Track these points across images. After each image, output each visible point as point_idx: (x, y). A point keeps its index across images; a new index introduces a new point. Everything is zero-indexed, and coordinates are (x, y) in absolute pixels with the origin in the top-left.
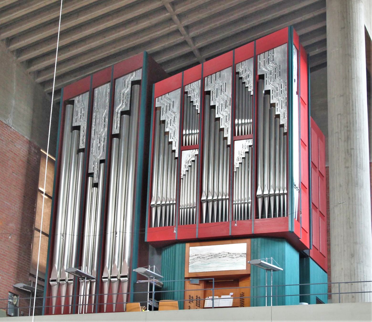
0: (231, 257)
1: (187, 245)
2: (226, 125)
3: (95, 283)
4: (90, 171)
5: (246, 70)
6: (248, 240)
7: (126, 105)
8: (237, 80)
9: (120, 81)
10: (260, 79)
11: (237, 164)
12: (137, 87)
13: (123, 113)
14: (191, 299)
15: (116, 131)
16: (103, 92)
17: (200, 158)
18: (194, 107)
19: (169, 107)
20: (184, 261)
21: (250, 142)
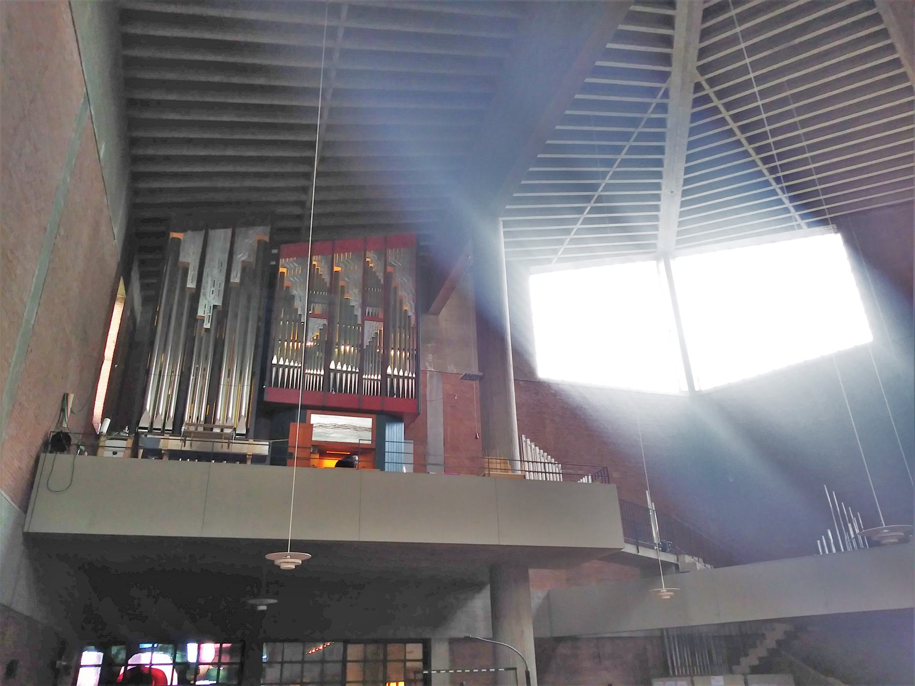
6: (374, 416)
7: (249, 256)
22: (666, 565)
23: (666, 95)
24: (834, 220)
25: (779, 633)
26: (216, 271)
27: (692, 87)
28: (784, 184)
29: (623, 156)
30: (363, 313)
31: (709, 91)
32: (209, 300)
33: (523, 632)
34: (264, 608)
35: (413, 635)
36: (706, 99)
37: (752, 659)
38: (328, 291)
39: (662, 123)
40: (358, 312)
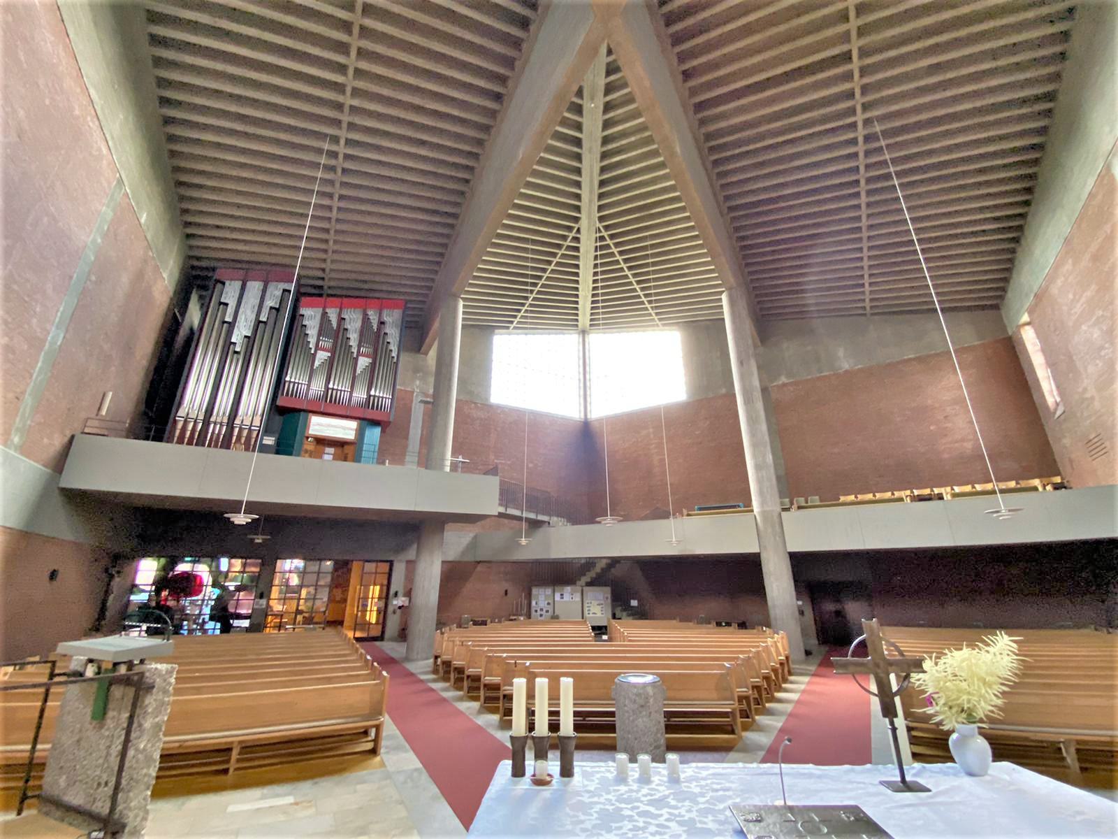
0: (344, 429)
1: (310, 414)
2: (354, 343)
4: (233, 340)
7: (276, 303)
8: (366, 320)
11: (358, 371)
13: (271, 308)
14: (306, 451)
15: (263, 318)
16: (254, 287)
19: (311, 317)
20: (306, 425)
21: (370, 360)
22: (543, 522)
23: (578, 231)
25: (603, 564)
26: (249, 312)
29: (552, 267)
31: (605, 234)
33: (433, 562)
34: (260, 541)
36: (602, 239)
38: (338, 335)
39: (577, 249)
40: (355, 350)
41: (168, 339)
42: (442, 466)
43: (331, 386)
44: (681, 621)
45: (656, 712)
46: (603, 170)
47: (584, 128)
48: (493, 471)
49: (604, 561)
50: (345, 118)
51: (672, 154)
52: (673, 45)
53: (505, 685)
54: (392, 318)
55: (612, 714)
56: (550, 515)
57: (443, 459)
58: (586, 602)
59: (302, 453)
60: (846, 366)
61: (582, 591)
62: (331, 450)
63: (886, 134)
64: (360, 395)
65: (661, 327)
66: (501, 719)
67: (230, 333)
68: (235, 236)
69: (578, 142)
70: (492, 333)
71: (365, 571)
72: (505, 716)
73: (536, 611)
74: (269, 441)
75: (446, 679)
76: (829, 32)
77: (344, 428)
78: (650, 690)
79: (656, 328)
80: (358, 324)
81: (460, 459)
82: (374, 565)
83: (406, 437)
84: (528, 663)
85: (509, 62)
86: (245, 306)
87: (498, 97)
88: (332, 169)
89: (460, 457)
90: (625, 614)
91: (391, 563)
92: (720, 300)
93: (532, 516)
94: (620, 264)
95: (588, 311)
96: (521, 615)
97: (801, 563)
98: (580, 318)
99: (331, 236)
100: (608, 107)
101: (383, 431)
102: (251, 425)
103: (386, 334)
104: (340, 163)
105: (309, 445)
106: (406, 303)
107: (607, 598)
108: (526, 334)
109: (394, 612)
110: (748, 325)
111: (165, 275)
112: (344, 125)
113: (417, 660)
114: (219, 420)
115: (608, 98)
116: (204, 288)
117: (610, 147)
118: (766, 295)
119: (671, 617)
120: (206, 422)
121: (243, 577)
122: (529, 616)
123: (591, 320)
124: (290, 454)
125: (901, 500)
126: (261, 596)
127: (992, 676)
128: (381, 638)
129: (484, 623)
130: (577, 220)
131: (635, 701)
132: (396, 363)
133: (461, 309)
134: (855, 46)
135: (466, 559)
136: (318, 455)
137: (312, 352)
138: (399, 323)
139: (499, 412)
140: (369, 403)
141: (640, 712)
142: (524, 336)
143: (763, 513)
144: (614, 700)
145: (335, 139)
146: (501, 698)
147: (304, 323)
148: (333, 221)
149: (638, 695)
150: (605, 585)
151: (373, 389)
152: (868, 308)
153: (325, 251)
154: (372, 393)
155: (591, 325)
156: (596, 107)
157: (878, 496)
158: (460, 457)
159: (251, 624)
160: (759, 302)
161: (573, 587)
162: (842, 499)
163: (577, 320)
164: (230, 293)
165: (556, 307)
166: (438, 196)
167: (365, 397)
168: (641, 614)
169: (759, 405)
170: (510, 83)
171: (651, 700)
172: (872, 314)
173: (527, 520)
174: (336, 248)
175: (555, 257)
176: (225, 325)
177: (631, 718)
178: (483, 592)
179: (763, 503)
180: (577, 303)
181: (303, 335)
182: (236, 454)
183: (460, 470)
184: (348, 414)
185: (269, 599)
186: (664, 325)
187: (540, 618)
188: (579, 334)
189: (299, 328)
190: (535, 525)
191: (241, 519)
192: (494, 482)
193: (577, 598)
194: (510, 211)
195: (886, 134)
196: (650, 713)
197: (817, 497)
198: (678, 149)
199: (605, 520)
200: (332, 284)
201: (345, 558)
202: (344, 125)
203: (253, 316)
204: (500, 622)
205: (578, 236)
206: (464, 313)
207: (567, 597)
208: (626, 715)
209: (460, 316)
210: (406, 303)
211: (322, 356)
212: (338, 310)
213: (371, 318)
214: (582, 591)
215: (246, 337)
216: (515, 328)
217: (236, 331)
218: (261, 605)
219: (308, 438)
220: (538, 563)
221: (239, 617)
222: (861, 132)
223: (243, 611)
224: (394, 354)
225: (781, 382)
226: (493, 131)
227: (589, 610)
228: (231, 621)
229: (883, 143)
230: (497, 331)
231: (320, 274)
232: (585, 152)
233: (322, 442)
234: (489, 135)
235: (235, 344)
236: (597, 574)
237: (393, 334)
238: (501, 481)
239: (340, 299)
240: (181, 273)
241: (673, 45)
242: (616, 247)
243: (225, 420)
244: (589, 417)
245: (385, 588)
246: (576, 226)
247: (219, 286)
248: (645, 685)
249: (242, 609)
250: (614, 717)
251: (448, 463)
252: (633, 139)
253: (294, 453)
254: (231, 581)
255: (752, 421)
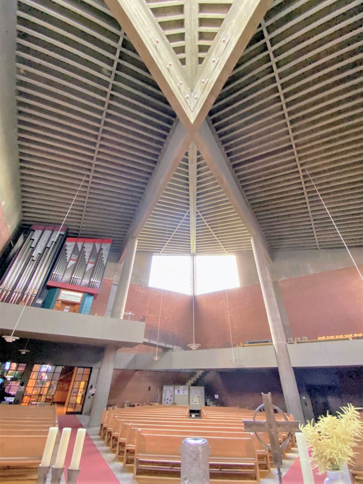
0: (76, 297)
1: (61, 289)
2: (87, 258)
3: (9, 292)
4: (33, 255)
5: (98, 246)
6: (83, 293)
9: (55, 232)
10: (101, 249)
11: (87, 270)
12: (61, 236)
14: (56, 307)
15: (48, 246)
16: (47, 233)
17: (76, 264)
18: (31, 240)
19: (70, 246)
20: (59, 294)
21: (93, 265)
22: (169, 349)
23: (189, 213)
24: (233, 252)
25: (200, 373)
26: (43, 243)
27: (196, 212)
28: (221, 241)
29: (178, 227)
30: (89, 261)
31: (200, 214)
32: (39, 250)
34: (24, 353)
35: (87, 366)
37: (191, 381)
38: (80, 254)
39: (189, 220)
40: (87, 261)
41: (5, 254)
42: (119, 316)
43: (73, 277)
44: (240, 407)
45: (203, 464)
46: (198, 189)
47: (189, 174)
48: (143, 320)
49: (201, 372)
50: (93, 168)
51: (222, 182)
52: (222, 144)
53: (128, 443)
54: (106, 247)
55: (179, 465)
56: (173, 345)
57: (120, 313)
58: (191, 395)
59: (55, 308)
60: (312, 272)
61: (189, 388)
62: (69, 307)
63: (312, 175)
64: (86, 281)
65: (227, 253)
66: (124, 465)
67: (33, 251)
68: (42, 212)
69: (187, 179)
70: (152, 255)
71: (78, 373)
72: (127, 463)
73: (165, 400)
74: (40, 302)
75: (103, 439)
76: (282, 139)
77: (76, 297)
78: (200, 449)
79: (224, 254)
80: (90, 249)
81: (130, 313)
82: (82, 369)
83: (107, 303)
84: (140, 429)
85: (159, 150)
86: (42, 240)
87: (155, 162)
88: (86, 187)
89: (130, 312)
90: (212, 403)
91: (91, 368)
92: (250, 242)
93: (163, 345)
94: (207, 226)
95: (195, 246)
96: (157, 402)
97: (301, 374)
98: (191, 249)
99: (84, 213)
100: (198, 167)
101: (95, 298)
102: (33, 294)
103: (102, 254)
104: (89, 185)
105: (58, 304)
106: (113, 241)
107: (202, 393)
108: (167, 255)
109: (89, 398)
110: (264, 252)
111: (9, 227)
112: (92, 171)
113: (93, 426)
114: (18, 291)
115: (199, 163)
116: (26, 233)
117: (200, 181)
118: (272, 240)
119: (235, 405)
120: (12, 292)
121: (15, 373)
122: (161, 402)
123: (196, 250)
124: (48, 308)
125: (348, 339)
126: (22, 384)
127: (347, 435)
128: (81, 413)
129: (133, 406)
130: (188, 208)
131: (191, 456)
132: (105, 267)
133: (136, 244)
134: (293, 143)
135: (130, 368)
136: (62, 309)
137: (68, 261)
138: (109, 249)
139: (152, 291)
140: (90, 285)
141: (194, 464)
142: (166, 256)
143: (278, 345)
144: (180, 455)
145: (88, 176)
146: (125, 452)
147: (66, 249)
148: (85, 207)
149: (193, 452)
150: (201, 385)
151: (92, 279)
152: (318, 246)
153: (81, 219)
154: (92, 280)
155: (196, 252)
156: (194, 166)
157: (337, 337)
158: (130, 312)
159: (15, 400)
160: (269, 243)
161: (185, 386)
162: (319, 338)
163: (190, 250)
164: (36, 235)
165: (180, 244)
166: (130, 198)
167: (88, 282)
168: (221, 403)
169: (272, 289)
170: (159, 158)
171: (201, 456)
172: (321, 249)
173: (159, 347)
174: (86, 218)
175: (179, 223)
176: (31, 249)
177: (189, 467)
178: (137, 387)
179: (277, 339)
180: (190, 242)
181: (65, 253)
182: (23, 308)
183: (129, 318)
184: (79, 290)
185: (26, 386)
186: (228, 252)
187: (167, 404)
188: (191, 256)
189: (64, 250)
190: (165, 349)
191: (10, 339)
192: (143, 324)
193: (186, 393)
194: (157, 204)
195: (312, 175)
196: (200, 464)
197: (306, 338)
198: (225, 180)
199: (192, 345)
200: (82, 232)
201: (71, 365)
202: (92, 171)
203: (45, 245)
204: (143, 405)
205: (189, 215)
206: (138, 246)
207: (181, 393)
208: (186, 465)
209: (136, 247)
210: (113, 241)
211: (72, 263)
212: (82, 243)
213: (97, 247)
214: (189, 388)
215: (39, 254)
216: (162, 253)
217: (35, 251)
218: (22, 389)
219: (58, 301)
220: (167, 372)
221: (9, 395)
222: (301, 175)
223: (12, 393)
224: (104, 263)
225: (283, 279)
226: (153, 175)
227: (192, 400)
228: (5, 398)
229: (311, 178)
230: (154, 254)
231: (78, 228)
232: (190, 183)
233: (65, 303)
234: (151, 176)
235: (33, 256)
236: (197, 379)
237: (105, 254)
238: (146, 326)
239: (84, 239)
240: (17, 226)
241: (222, 144)
242: (205, 219)
243: (21, 291)
244: (195, 294)
245: (87, 383)
246: (188, 211)
247: (32, 232)
248: (197, 445)
249: (11, 392)
250: (180, 467)
251: (122, 315)
252: (209, 178)
253: (50, 308)
254: (10, 375)
255: (269, 296)
